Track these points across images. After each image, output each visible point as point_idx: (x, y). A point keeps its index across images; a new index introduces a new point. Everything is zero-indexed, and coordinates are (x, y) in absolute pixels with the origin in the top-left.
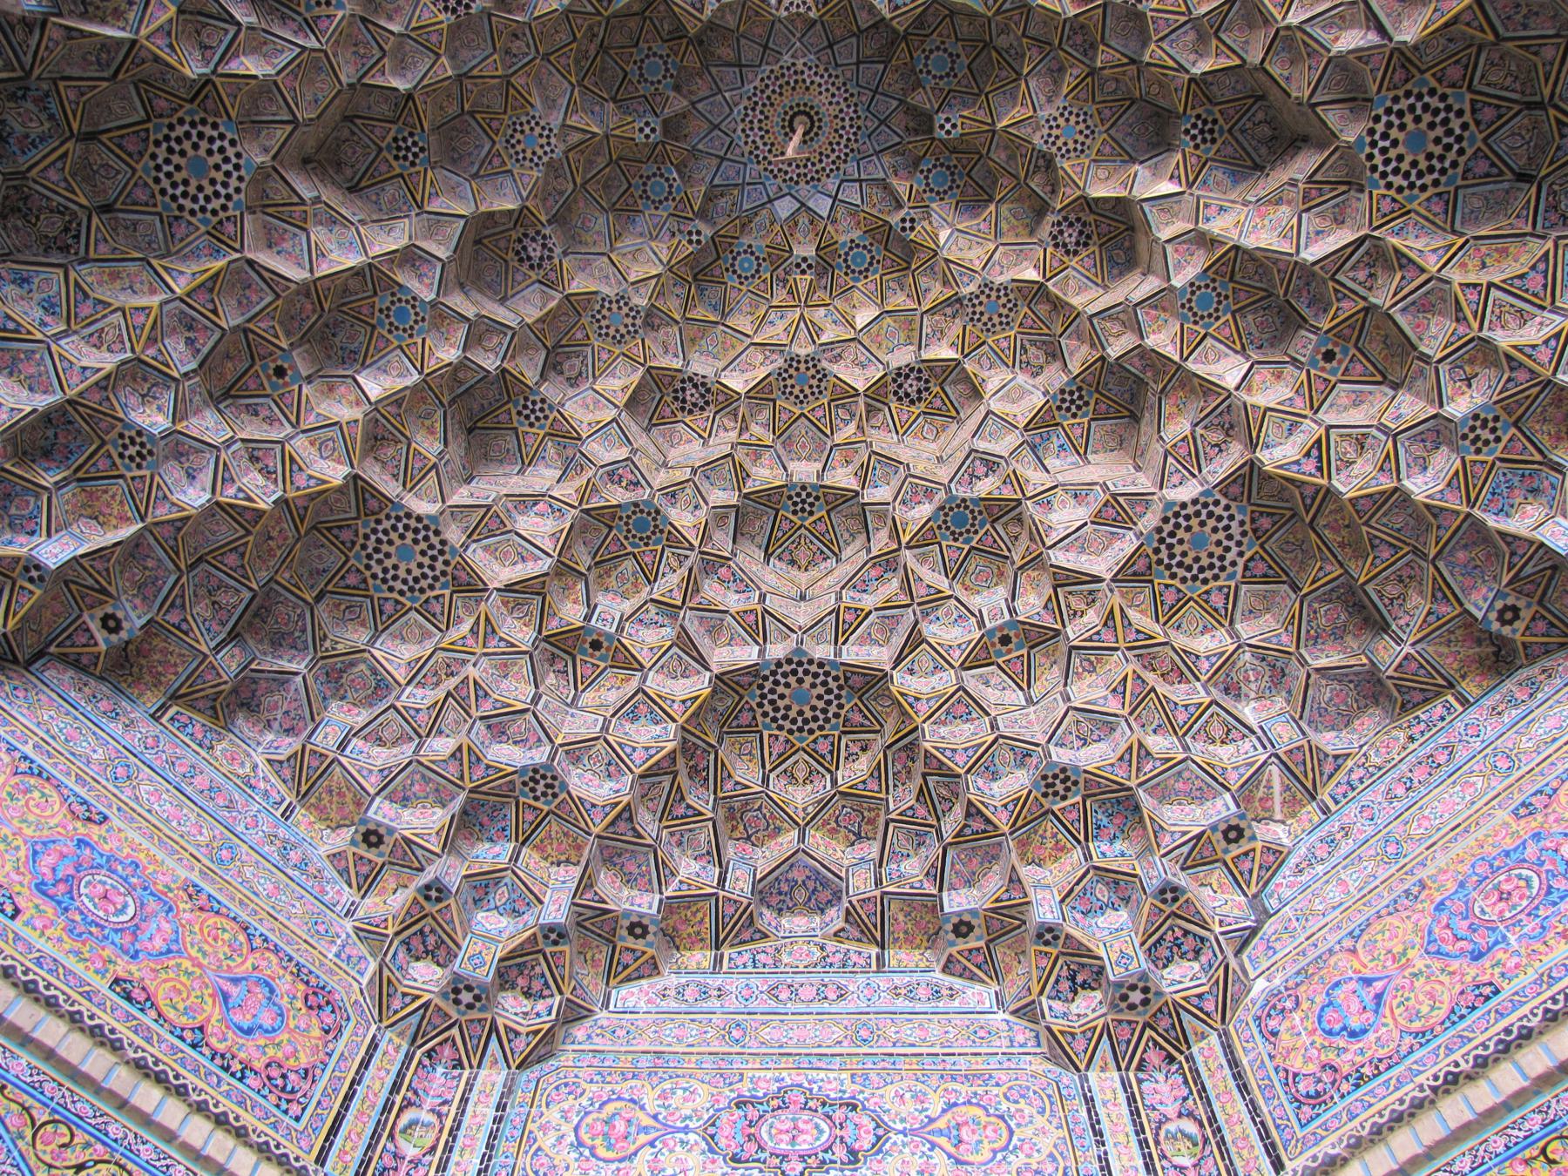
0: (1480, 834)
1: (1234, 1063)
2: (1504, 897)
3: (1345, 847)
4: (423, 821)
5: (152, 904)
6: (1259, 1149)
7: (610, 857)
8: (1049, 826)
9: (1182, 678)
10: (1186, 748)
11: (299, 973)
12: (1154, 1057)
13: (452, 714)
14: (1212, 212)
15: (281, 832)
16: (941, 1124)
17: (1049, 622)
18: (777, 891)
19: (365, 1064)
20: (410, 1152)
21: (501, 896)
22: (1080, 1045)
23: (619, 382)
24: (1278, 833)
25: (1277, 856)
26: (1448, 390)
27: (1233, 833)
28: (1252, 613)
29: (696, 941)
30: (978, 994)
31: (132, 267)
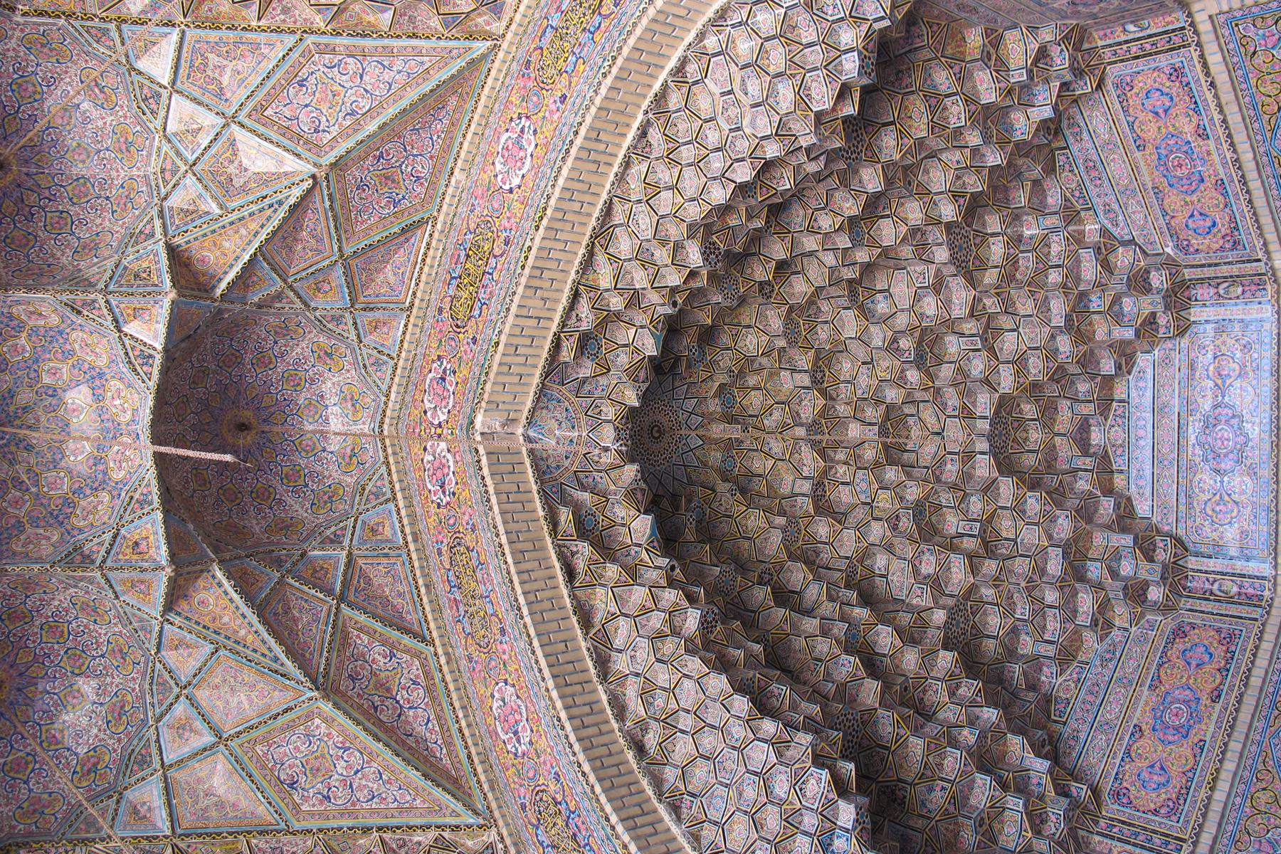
0: (1142, 163)
1: (1203, 266)
2: (1180, 166)
3: (1116, 207)
4: (1086, 602)
5: (1169, 699)
6: (1248, 265)
7: (1089, 521)
8: (1082, 328)
9: (1017, 262)
10: (1058, 266)
11: (1170, 642)
12: (1186, 294)
13: (1036, 593)
14: (816, 225)
15: (1098, 663)
16: (1219, 382)
17: (984, 320)
18: (1084, 446)
19: (1202, 612)
20: (1235, 589)
21: (1114, 564)
22: (1181, 323)
23: (822, 529)
24: (1091, 228)
25: (1104, 232)
26: (963, 144)
27: (1098, 250)
28: (984, 225)
29: (1111, 481)
30: (1143, 360)
31: (897, 759)
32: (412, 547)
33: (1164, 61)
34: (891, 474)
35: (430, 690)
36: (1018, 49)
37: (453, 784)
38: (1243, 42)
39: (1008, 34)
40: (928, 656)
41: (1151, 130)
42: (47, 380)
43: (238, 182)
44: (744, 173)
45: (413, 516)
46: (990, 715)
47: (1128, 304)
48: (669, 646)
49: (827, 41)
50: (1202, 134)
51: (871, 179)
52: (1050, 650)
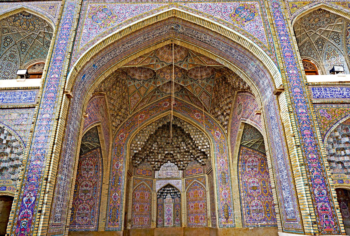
4: (153, 163)
11: (150, 170)
25: (189, 163)
32: (157, 100)
33: (203, 171)
34: (165, 144)
35: (143, 105)
36: (204, 160)
37: (134, 111)
38: (203, 178)
40: (149, 151)
41: (197, 169)
42: (176, 69)
43: (197, 89)
44: (194, 139)
45: (161, 100)
46: (144, 157)
47: (182, 165)
48: (150, 132)
49: (205, 148)
50: (196, 173)
51: (194, 146)
52: (148, 160)
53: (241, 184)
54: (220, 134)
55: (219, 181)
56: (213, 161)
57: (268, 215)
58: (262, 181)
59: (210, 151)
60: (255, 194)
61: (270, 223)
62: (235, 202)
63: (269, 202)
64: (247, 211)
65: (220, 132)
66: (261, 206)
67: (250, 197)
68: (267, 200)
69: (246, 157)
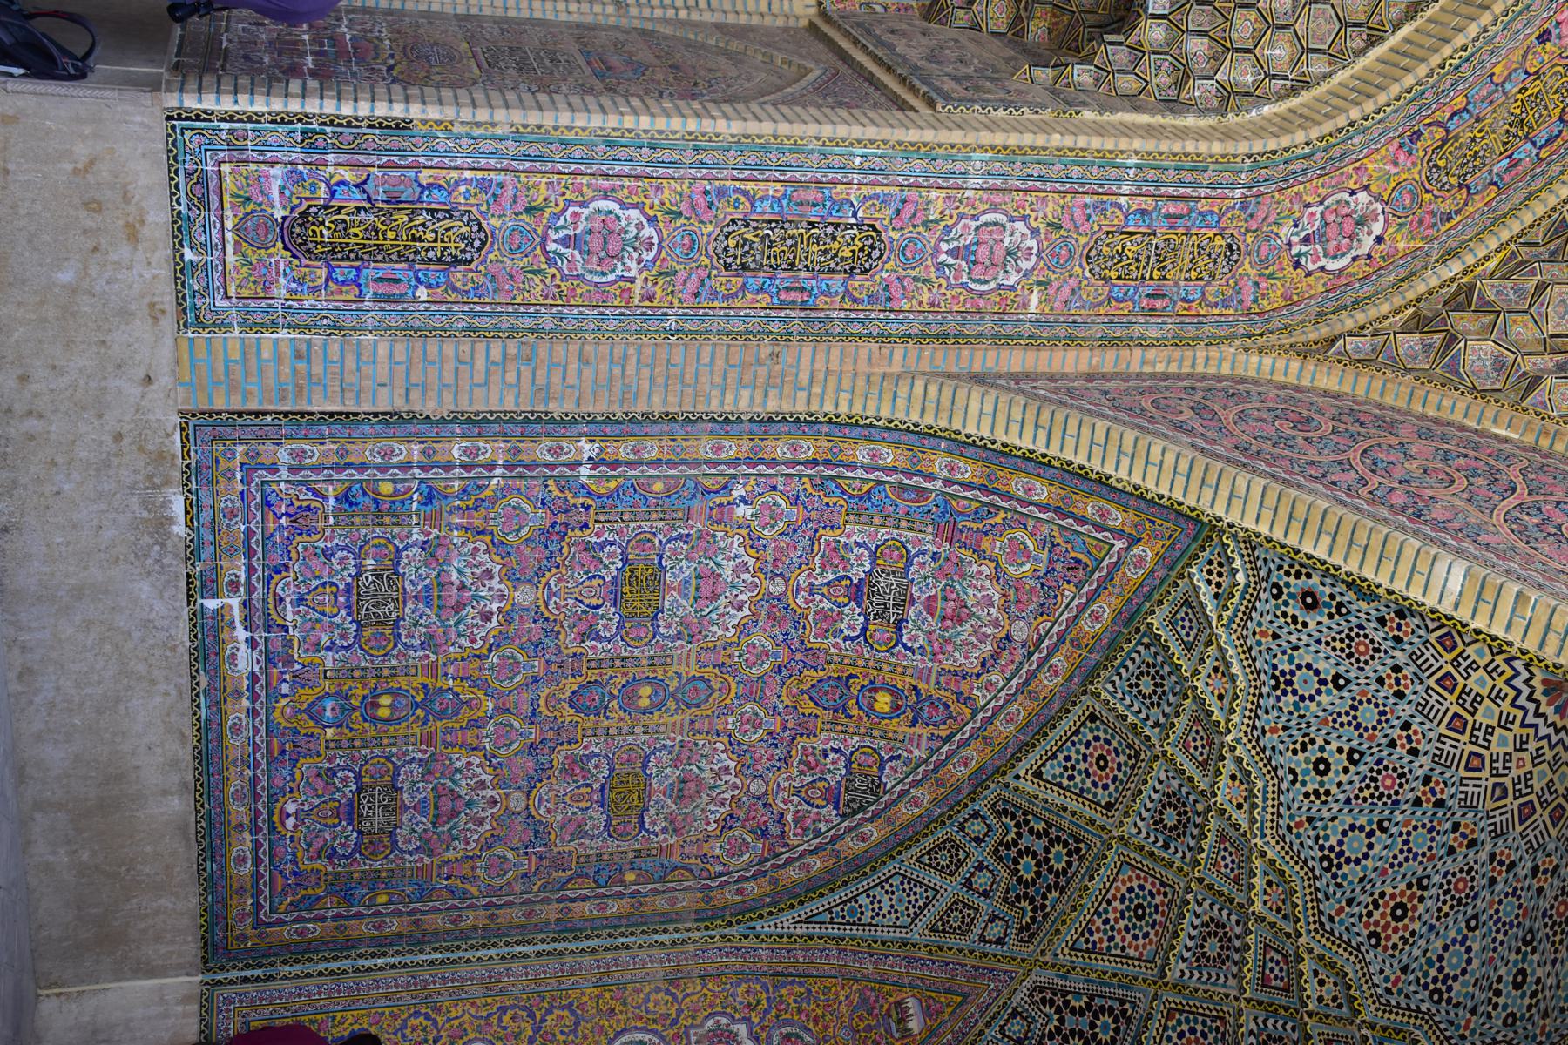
39: (1003, 28)
53: (704, 448)
54: (1334, 265)
55: (773, 189)
56: (1027, 139)
57: (329, 704)
58: (709, 672)
59: (1134, 102)
60: (571, 589)
61: (238, 710)
62: (496, 353)
63: (476, 724)
64: (386, 488)
65: (1360, 269)
66: (429, 642)
67: (546, 533)
68: (502, 709)
69: (1018, 551)
